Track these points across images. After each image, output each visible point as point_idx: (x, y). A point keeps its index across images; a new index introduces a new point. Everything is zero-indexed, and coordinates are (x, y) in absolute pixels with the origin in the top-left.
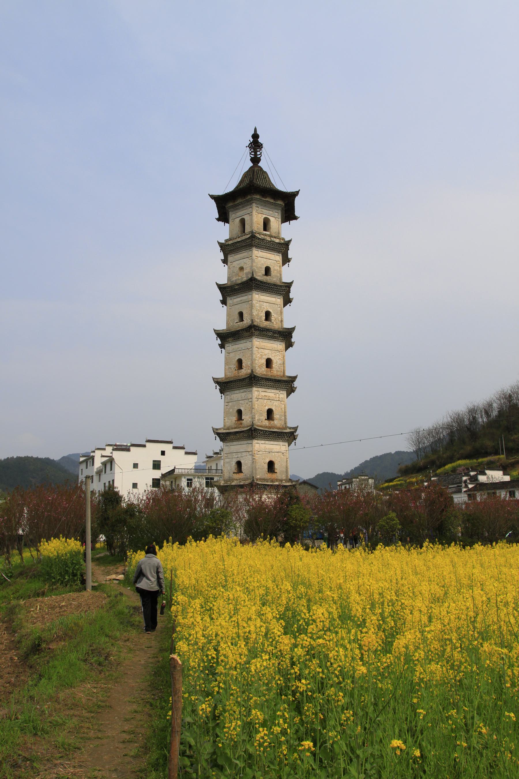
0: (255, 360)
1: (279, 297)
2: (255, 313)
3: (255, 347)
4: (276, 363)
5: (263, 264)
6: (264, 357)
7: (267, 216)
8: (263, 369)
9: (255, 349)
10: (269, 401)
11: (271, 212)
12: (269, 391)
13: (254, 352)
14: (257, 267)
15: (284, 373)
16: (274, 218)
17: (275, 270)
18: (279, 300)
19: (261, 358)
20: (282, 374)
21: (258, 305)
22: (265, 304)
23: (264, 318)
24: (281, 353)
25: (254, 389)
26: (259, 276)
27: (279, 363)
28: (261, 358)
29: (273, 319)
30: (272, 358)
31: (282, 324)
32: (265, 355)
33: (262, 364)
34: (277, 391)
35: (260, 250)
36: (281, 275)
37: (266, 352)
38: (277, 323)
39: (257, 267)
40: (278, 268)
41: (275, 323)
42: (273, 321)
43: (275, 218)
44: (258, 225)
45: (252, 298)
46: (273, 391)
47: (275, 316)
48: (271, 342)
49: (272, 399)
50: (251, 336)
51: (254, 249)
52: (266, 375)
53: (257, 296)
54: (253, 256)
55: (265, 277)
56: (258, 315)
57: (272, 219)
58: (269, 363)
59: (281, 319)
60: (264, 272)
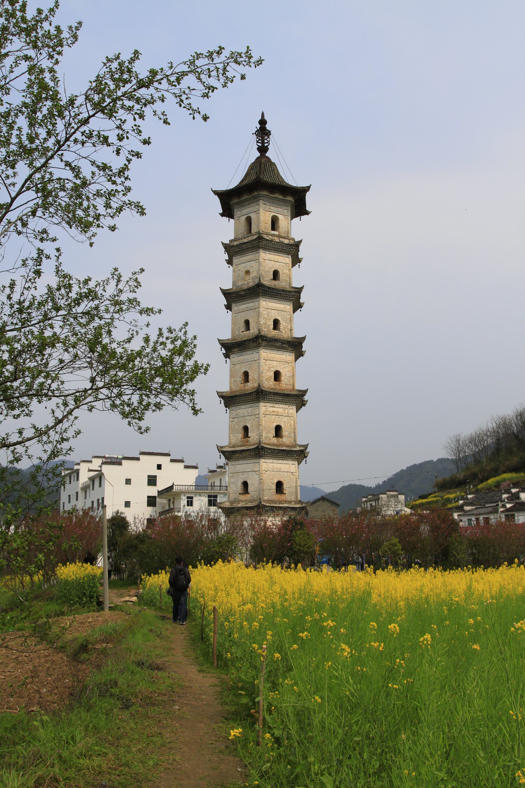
5: (270, 268)
6: (272, 369)
9: (262, 361)
12: (277, 406)
15: (294, 386)
17: (284, 274)
18: (288, 307)
21: (265, 312)
22: (273, 311)
23: (272, 326)
25: (262, 404)
26: (266, 281)
27: (288, 375)
28: (269, 370)
30: (281, 371)
34: (286, 406)
35: (267, 252)
36: (290, 279)
37: (275, 363)
46: (281, 406)
48: (280, 353)
52: (274, 389)
57: (280, 217)
58: (277, 375)
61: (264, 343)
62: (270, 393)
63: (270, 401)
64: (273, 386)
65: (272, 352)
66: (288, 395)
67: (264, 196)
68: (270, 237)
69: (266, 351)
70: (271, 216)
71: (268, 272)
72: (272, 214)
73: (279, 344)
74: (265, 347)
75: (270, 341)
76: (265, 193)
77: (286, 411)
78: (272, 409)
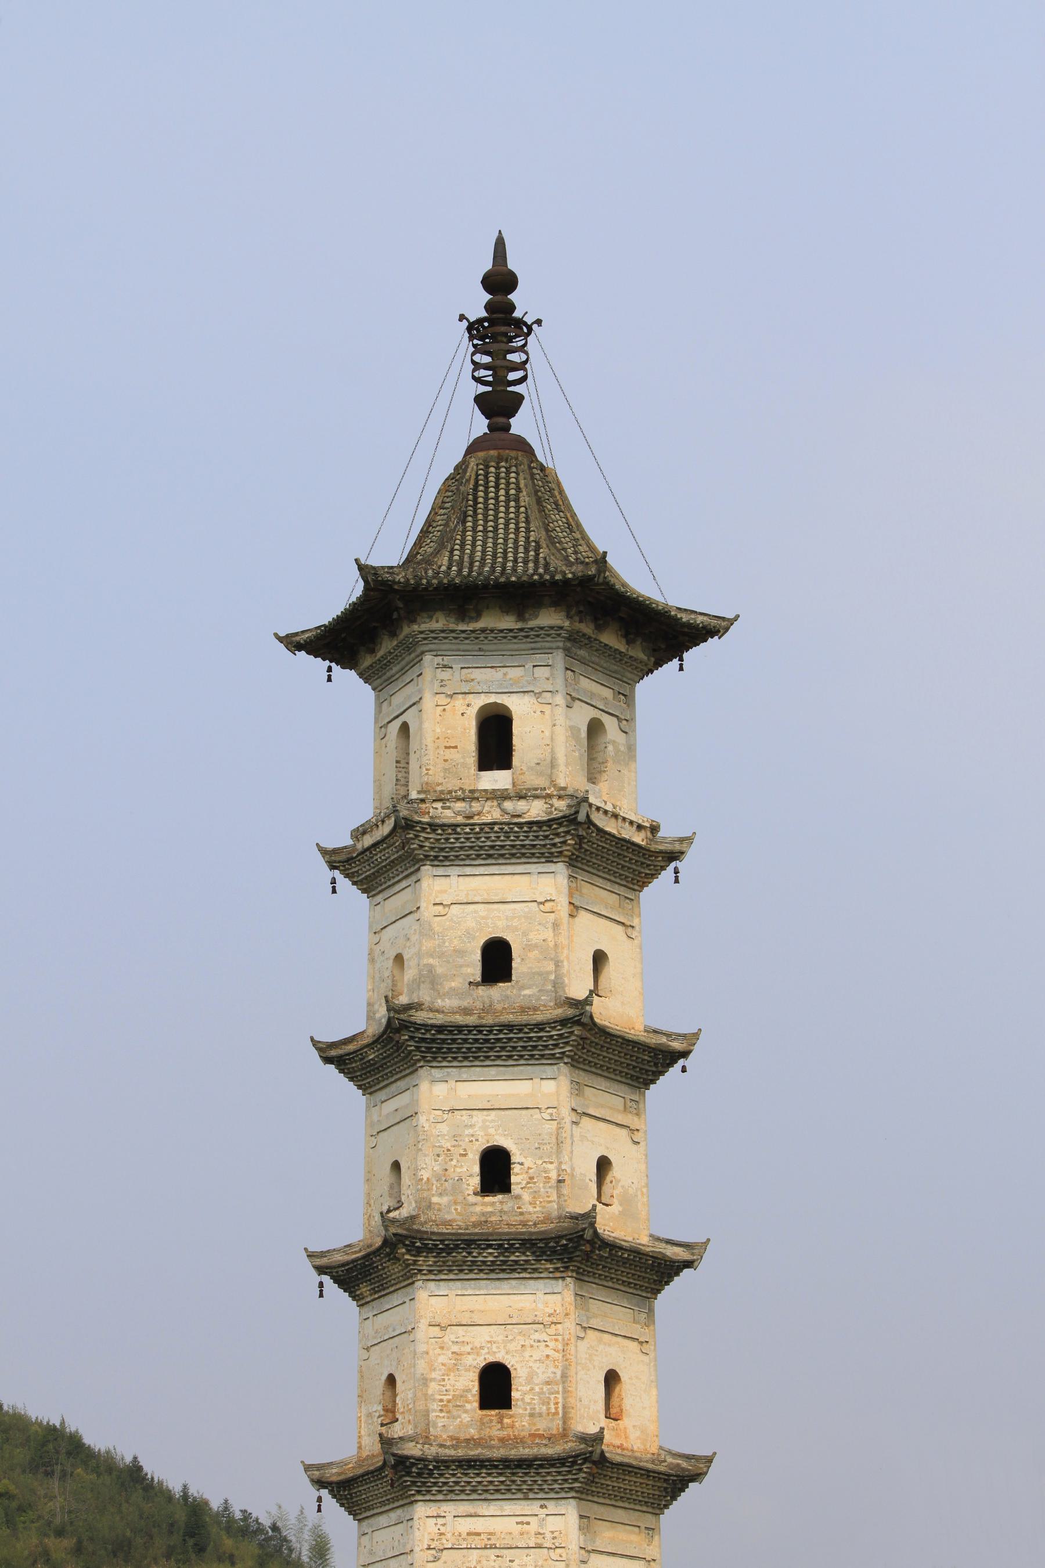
0: (425, 1381)
1: (550, 1071)
2: (428, 1167)
3: (423, 1325)
4: (530, 1379)
5: (469, 935)
6: (469, 1360)
7: (492, 699)
8: (466, 1418)
9: (423, 1332)
10: (491, 1553)
11: (514, 673)
12: (492, 1508)
13: (421, 1348)
14: (441, 955)
15: (565, 1419)
16: (527, 699)
17: (529, 947)
18: (549, 1086)
19: (454, 1368)
20: (555, 1426)
21: (444, 1128)
22: (478, 1117)
23: (476, 1181)
24: (552, 1330)
25: (421, 1510)
26: (453, 992)
27: (542, 1377)
28: (454, 1368)
29: (516, 1178)
30: (509, 1362)
31: (560, 1195)
32: (476, 1351)
33: (462, 1396)
34: (534, 1507)
35: (454, 871)
36: (558, 964)
37: (482, 1335)
38: (536, 1194)
39: (441, 955)
40: (549, 934)
41: (526, 1197)
42: (515, 1189)
43: (538, 695)
44: (450, 754)
45: (415, 1102)
46: (509, 1507)
47: (528, 1162)
48: (505, 1286)
49: (509, 1542)
50: (408, 1278)
51: (427, 870)
52: (477, 1442)
53: (440, 1090)
54: (423, 905)
55: (482, 991)
56: (443, 1176)
57: (519, 707)
58: (495, 1386)
59: (560, 1170)
60: (476, 971)
61: (426, 1261)
62: (443, 1464)
63: (451, 1493)
64: (473, 1432)
65: (470, 1288)
66: (524, 1464)
67: (435, 636)
68: (459, 806)
69: (443, 1288)
70: (473, 712)
71: (460, 953)
72: (480, 702)
73: (490, 1255)
74: (436, 1273)
75: (449, 1250)
76: (438, 622)
77: (534, 1525)
78: (465, 1525)
